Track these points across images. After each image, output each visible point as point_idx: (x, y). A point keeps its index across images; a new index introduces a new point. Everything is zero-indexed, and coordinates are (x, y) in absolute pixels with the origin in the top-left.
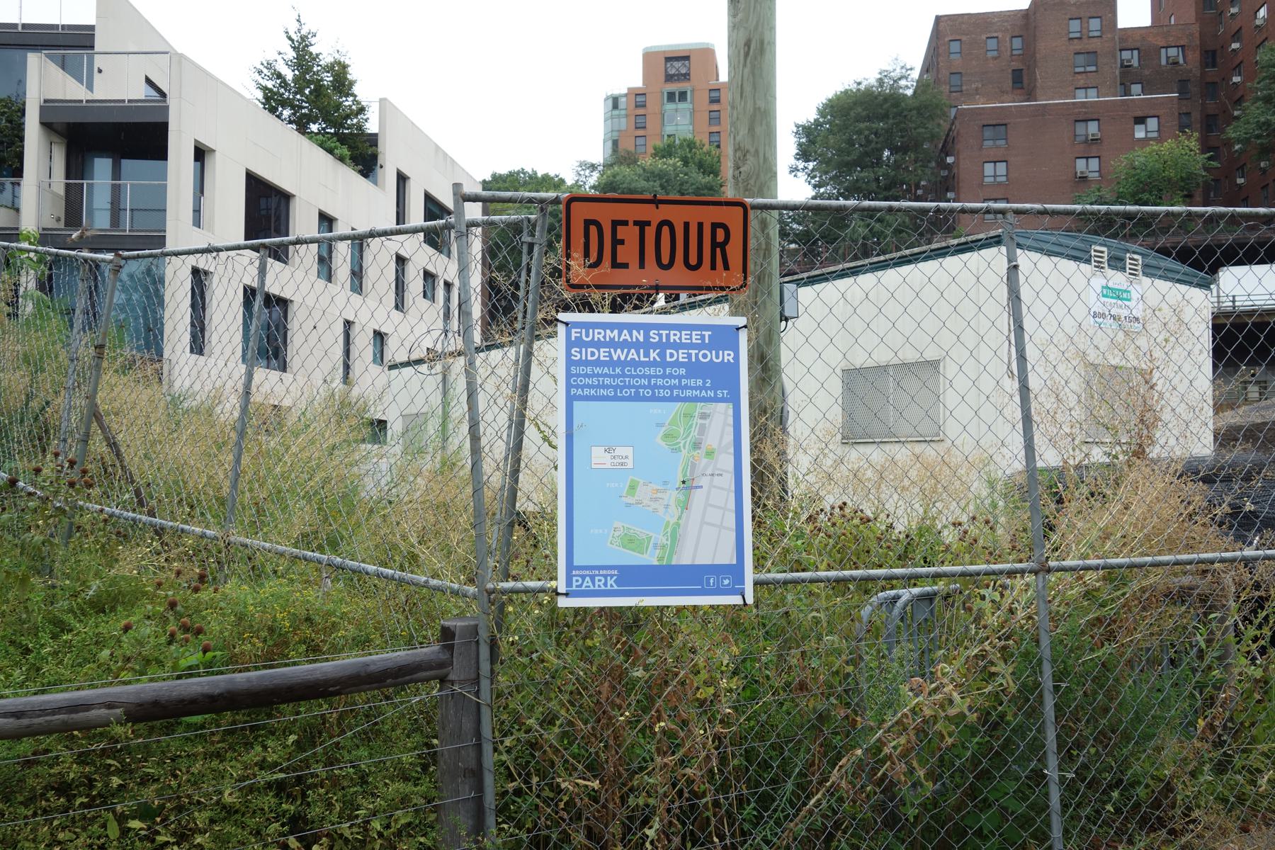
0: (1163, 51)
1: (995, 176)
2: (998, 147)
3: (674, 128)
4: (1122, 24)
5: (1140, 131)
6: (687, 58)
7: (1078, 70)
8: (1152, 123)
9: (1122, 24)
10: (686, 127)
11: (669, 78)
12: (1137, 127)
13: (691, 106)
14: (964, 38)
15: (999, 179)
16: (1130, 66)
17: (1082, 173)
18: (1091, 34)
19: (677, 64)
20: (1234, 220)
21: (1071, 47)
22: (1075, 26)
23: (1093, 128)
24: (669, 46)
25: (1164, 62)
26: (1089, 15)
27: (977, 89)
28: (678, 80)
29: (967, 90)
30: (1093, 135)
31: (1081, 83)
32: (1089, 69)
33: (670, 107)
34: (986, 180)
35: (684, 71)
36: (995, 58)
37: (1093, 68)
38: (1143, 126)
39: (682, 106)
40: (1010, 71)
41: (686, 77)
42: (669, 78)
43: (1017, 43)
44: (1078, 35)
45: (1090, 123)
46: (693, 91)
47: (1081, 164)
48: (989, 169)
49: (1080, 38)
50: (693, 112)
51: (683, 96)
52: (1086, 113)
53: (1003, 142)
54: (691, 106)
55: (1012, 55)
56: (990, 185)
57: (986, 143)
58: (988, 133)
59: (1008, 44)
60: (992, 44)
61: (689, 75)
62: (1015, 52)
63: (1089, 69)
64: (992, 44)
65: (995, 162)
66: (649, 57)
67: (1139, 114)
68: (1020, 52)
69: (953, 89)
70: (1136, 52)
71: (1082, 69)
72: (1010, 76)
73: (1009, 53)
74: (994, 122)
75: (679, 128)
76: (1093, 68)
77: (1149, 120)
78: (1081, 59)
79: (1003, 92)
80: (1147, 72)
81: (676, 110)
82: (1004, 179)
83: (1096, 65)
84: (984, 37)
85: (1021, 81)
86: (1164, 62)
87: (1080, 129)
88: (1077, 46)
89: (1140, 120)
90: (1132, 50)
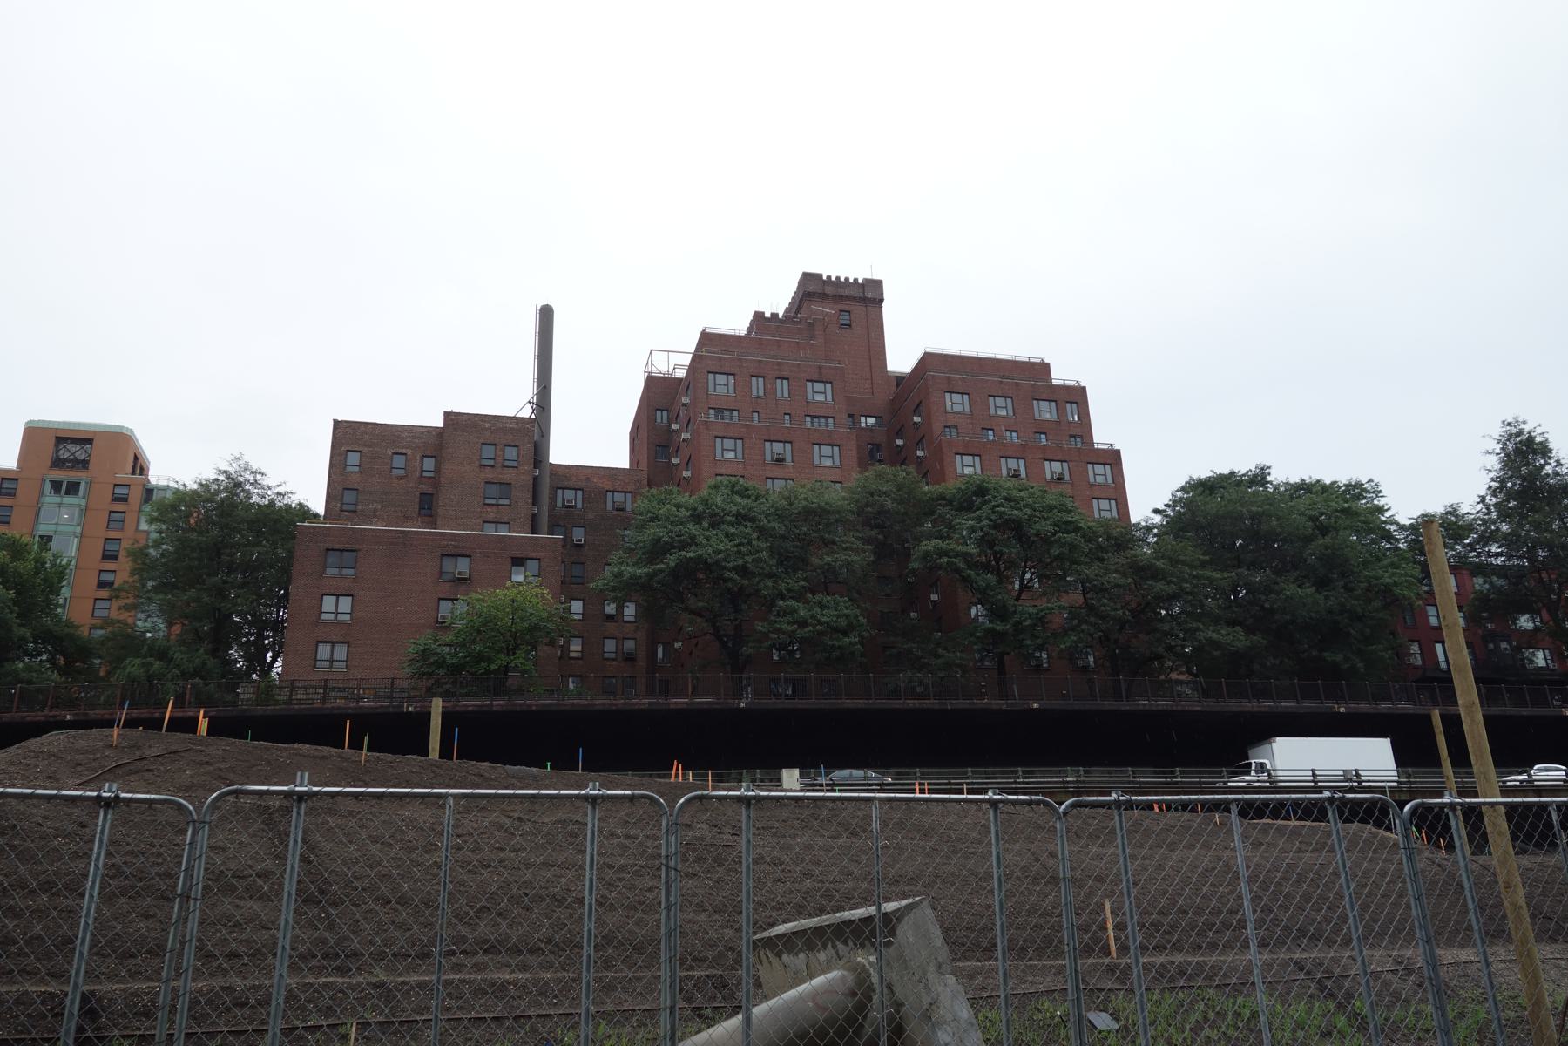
0: (610, 494)
1: (336, 613)
2: (345, 577)
3: (53, 528)
4: (628, 467)
5: (518, 573)
6: (89, 441)
7: (488, 501)
8: (533, 566)
9: (628, 467)
10: (71, 529)
11: (58, 463)
12: (514, 568)
13: (83, 502)
14: (365, 450)
15: (341, 617)
16: (571, 507)
17: (443, 617)
18: (507, 463)
19: (73, 447)
20: (853, 703)
21: (483, 475)
22: (488, 452)
23: (463, 566)
24: (65, 423)
25: (609, 506)
26: (505, 442)
27: (375, 511)
28: (73, 467)
29: (362, 510)
30: (460, 573)
31: (491, 516)
32: (502, 502)
33: (50, 499)
34: (324, 616)
35: (81, 456)
36: (401, 478)
37: (506, 502)
38: (523, 569)
39: (68, 500)
40: (418, 494)
41: (85, 464)
42: (58, 463)
43: (429, 464)
44: (492, 463)
45: (459, 558)
46: (90, 483)
47: (445, 606)
48: (329, 603)
49: (493, 466)
50: (85, 510)
51: (73, 488)
52: (456, 547)
53: (351, 572)
54: (83, 502)
55: (421, 476)
56: (327, 624)
57: (330, 571)
58: (332, 559)
59: (418, 463)
60: (399, 461)
61: (88, 462)
62: (425, 474)
63: (502, 502)
64: (399, 461)
65: (338, 596)
66: (33, 434)
67: (518, 554)
68: (432, 474)
69: (345, 507)
70: (580, 493)
71: (493, 501)
72: (417, 500)
73: (418, 474)
74: (341, 547)
75: (61, 528)
76: (506, 502)
77: (528, 561)
78: (493, 490)
79: (407, 518)
80: (590, 515)
81: (60, 505)
82: (348, 617)
83: (509, 498)
84: (390, 452)
85: (427, 507)
86: (609, 506)
87: (448, 565)
88: (489, 474)
89: (519, 562)
90: (576, 489)
